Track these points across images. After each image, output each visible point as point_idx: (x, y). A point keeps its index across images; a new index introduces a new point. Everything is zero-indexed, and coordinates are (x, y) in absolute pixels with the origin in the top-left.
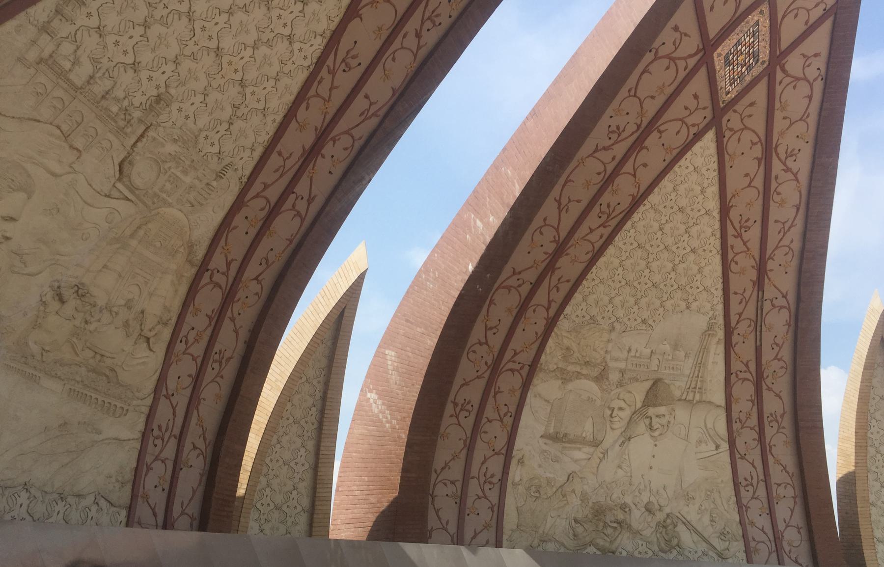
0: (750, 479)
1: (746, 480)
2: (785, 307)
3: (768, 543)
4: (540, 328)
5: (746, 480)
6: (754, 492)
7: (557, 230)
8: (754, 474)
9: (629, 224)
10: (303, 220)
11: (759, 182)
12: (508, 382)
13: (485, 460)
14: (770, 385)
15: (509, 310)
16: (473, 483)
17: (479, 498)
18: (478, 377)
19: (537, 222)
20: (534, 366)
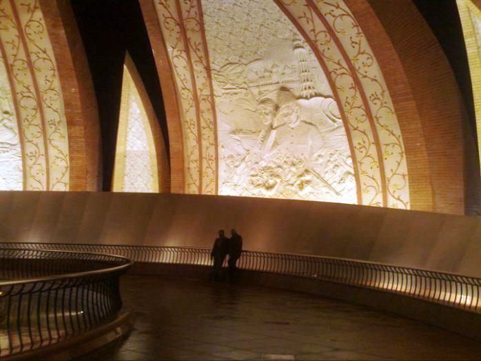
0: (362, 143)
1: (359, 144)
2: (344, 15)
3: (377, 187)
5: (359, 144)
6: (367, 153)
7: (172, 18)
8: (366, 140)
10: (50, 60)
12: (204, 106)
13: (207, 148)
14: (365, 74)
15: (185, 67)
17: (207, 167)
18: (191, 106)
19: (162, 19)
20: (212, 95)
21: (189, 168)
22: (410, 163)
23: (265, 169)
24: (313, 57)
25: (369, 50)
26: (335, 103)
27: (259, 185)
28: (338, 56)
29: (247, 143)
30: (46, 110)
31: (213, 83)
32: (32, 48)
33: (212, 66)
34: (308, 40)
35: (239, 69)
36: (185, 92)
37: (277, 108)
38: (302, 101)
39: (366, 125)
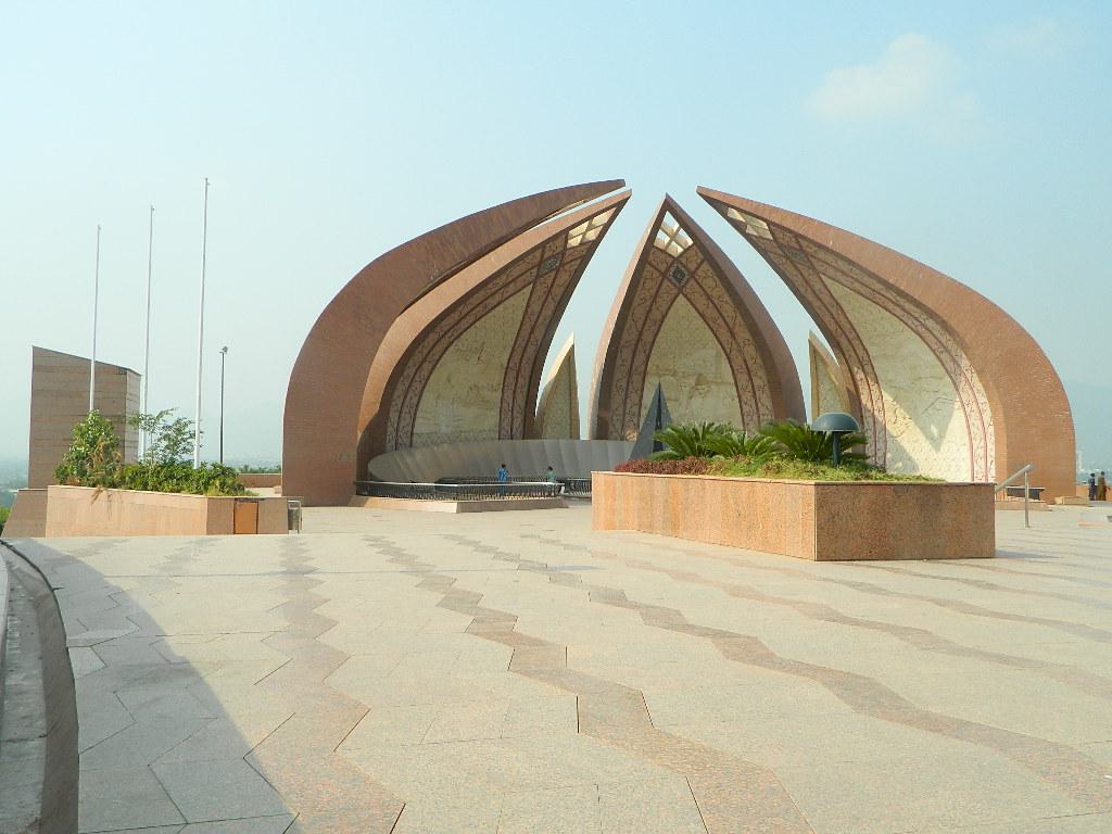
11: (711, 305)
12: (636, 378)
16: (627, 416)
19: (627, 326)
32: (532, 339)
34: (725, 352)
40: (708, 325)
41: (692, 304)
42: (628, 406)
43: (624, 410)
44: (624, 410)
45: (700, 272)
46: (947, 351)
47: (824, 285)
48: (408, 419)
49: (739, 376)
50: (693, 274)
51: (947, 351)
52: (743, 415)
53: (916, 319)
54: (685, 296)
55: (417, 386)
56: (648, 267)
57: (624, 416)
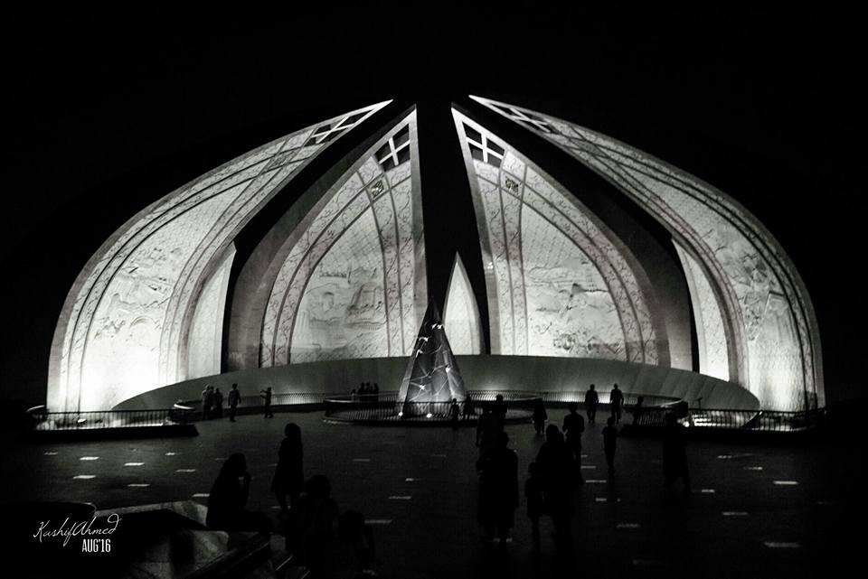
4: (519, 272)
9: (522, 236)
11: (557, 212)
19: (492, 242)
21: (504, 334)
22: (656, 334)
23: (564, 335)
24: (595, 268)
25: (628, 268)
26: (609, 295)
27: (560, 347)
28: (610, 269)
29: (550, 318)
30: (403, 297)
31: (526, 278)
32: (402, 261)
33: (524, 268)
35: (544, 271)
36: (504, 283)
37: (572, 296)
38: (588, 293)
39: (629, 310)
40: (564, 233)
41: (539, 213)
42: (516, 321)
43: (513, 323)
44: (513, 323)
45: (528, 180)
46: (757, 236)
47: (632, 177)
48: (284, 341)
49: (611, 283)
50: (524, 182)
51: (757, 236)
52: (622, 324)
53: (716, 201)
54: (529, 205)
55: (288, 311)
56: (481, 182)
57: (514, 330)
